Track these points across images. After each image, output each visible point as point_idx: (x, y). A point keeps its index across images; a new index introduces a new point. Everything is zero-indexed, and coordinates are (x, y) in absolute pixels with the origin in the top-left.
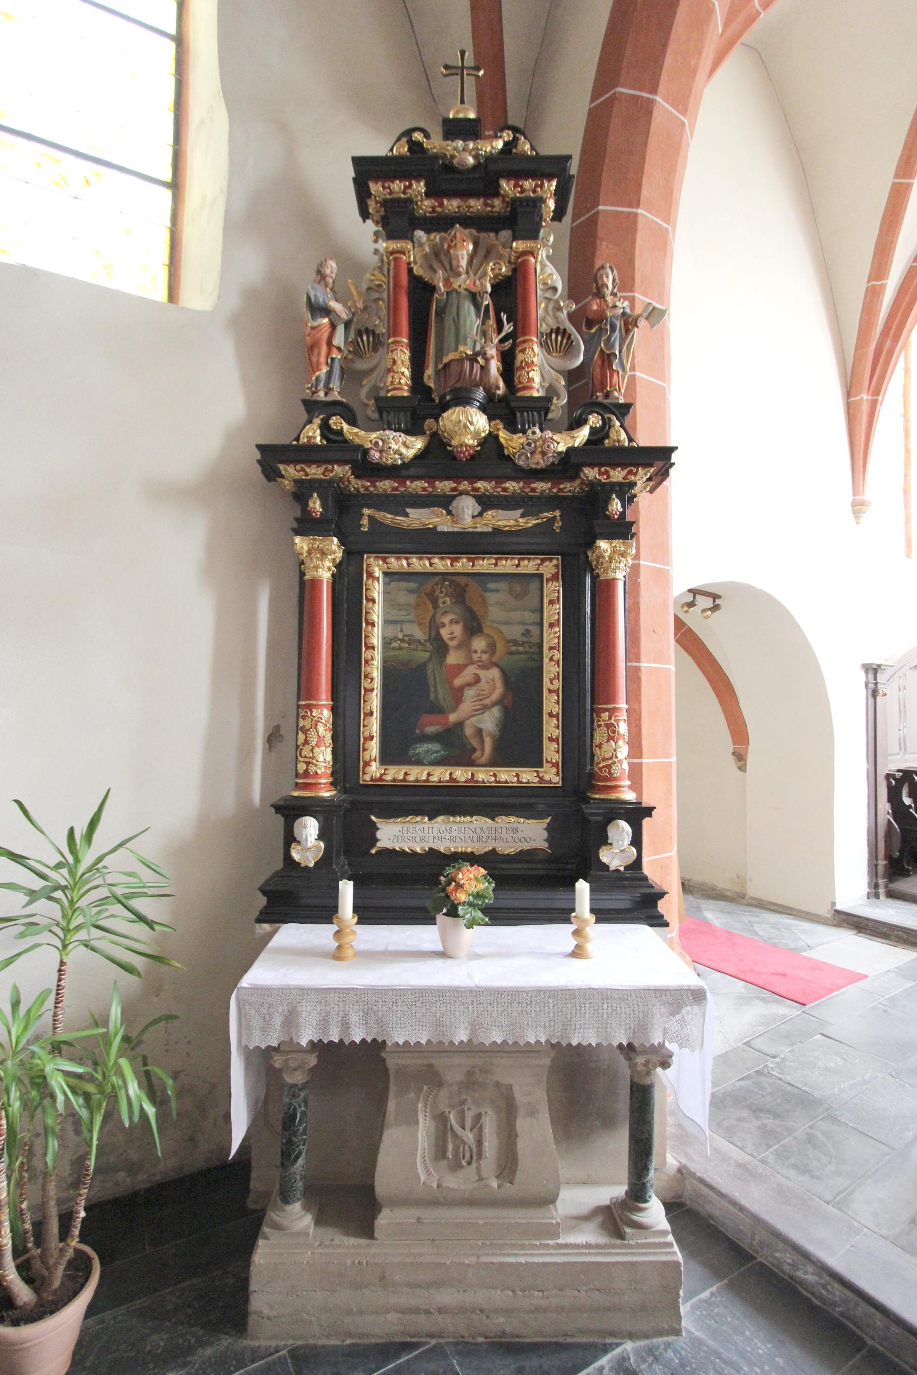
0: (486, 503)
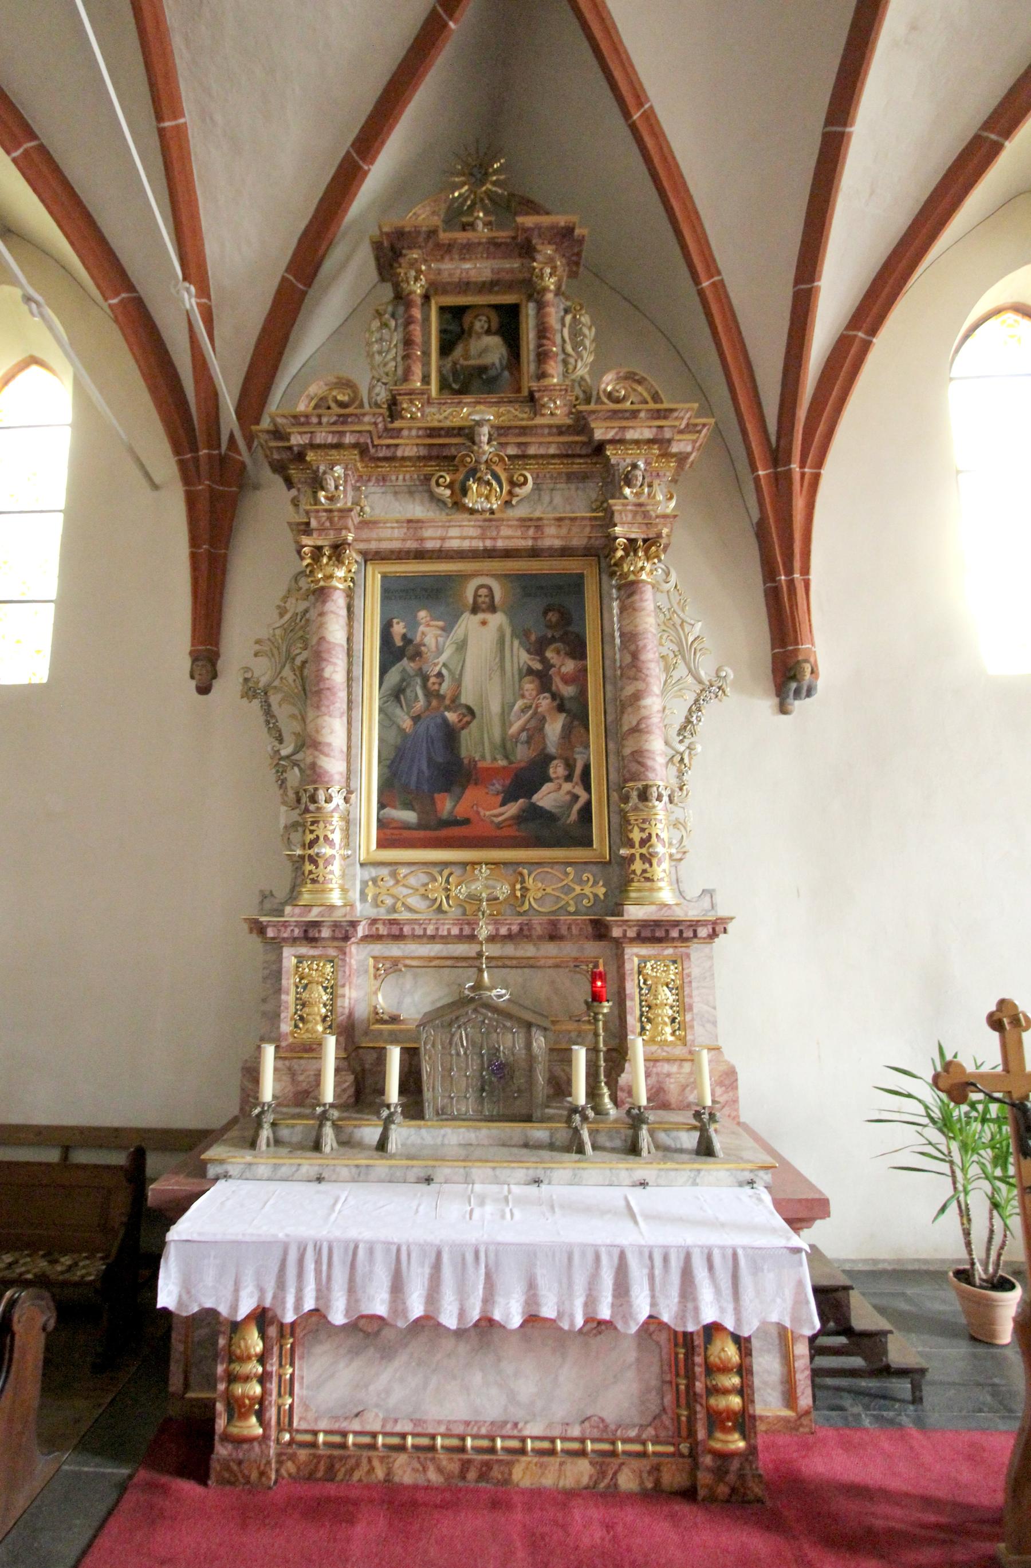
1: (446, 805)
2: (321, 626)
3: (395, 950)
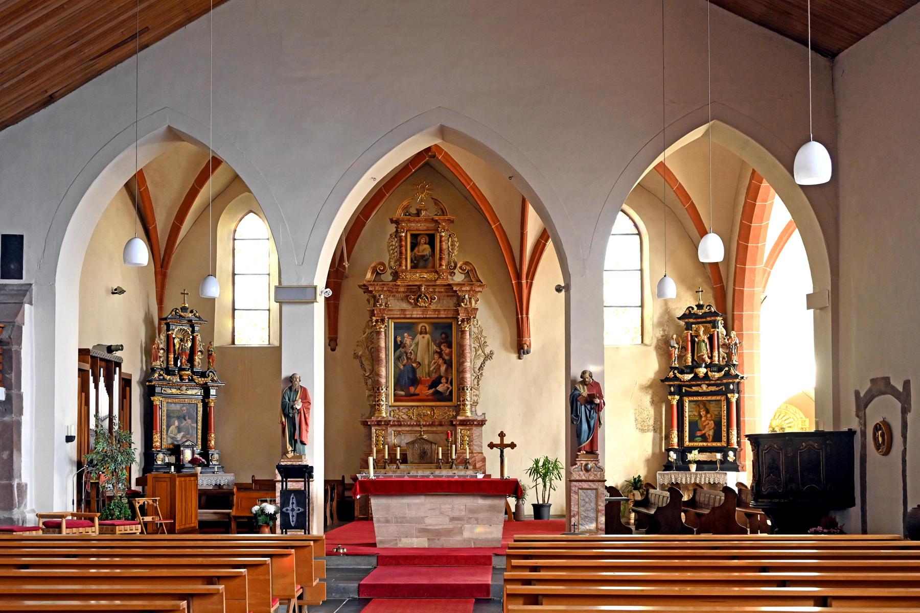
0: (709, 385)
1: (412, 390)
2: (379, 342)
3: (399, 429)
